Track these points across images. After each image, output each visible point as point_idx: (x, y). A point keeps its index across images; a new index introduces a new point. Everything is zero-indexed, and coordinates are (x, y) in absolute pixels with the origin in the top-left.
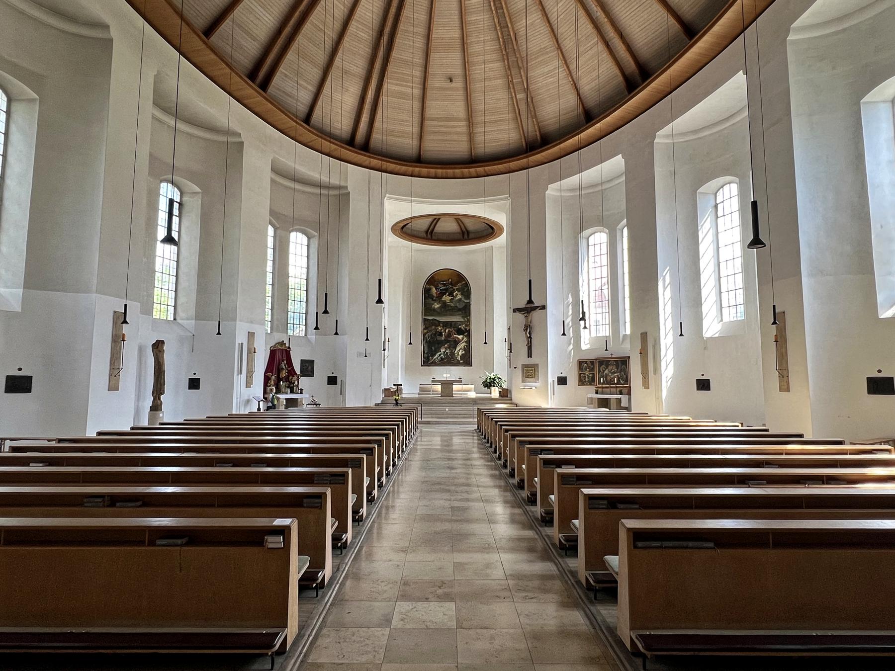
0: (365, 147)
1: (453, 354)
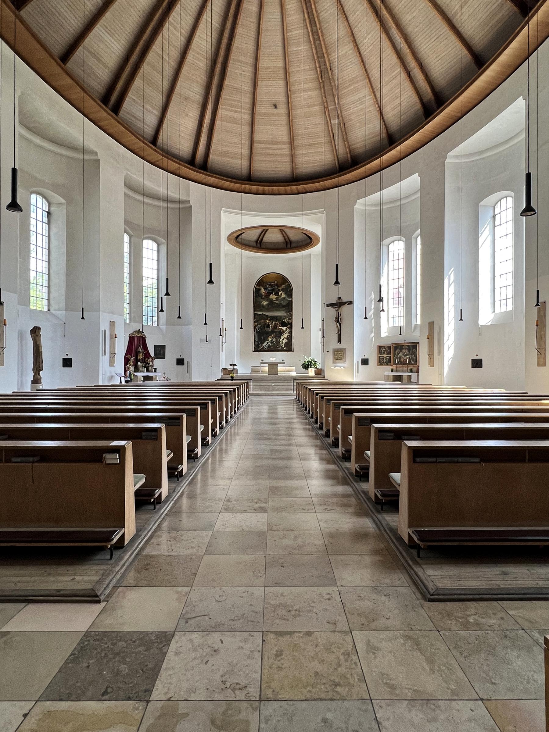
1: (278, 342)
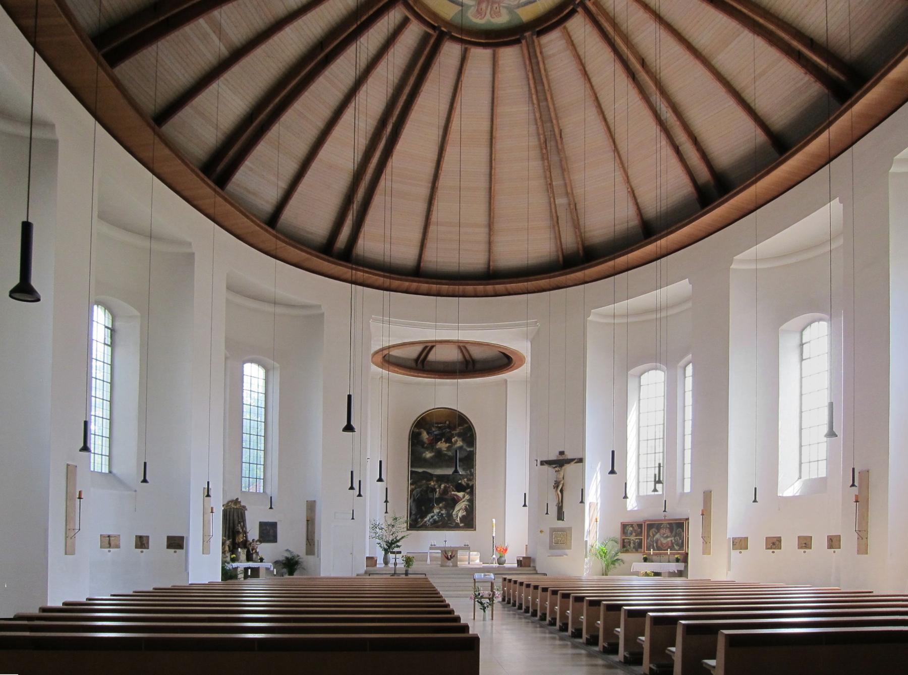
0: (347, 256)
1: (450, 516)
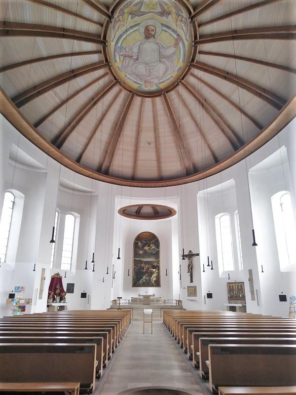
0: (107, 173)
1: (150, 280)
